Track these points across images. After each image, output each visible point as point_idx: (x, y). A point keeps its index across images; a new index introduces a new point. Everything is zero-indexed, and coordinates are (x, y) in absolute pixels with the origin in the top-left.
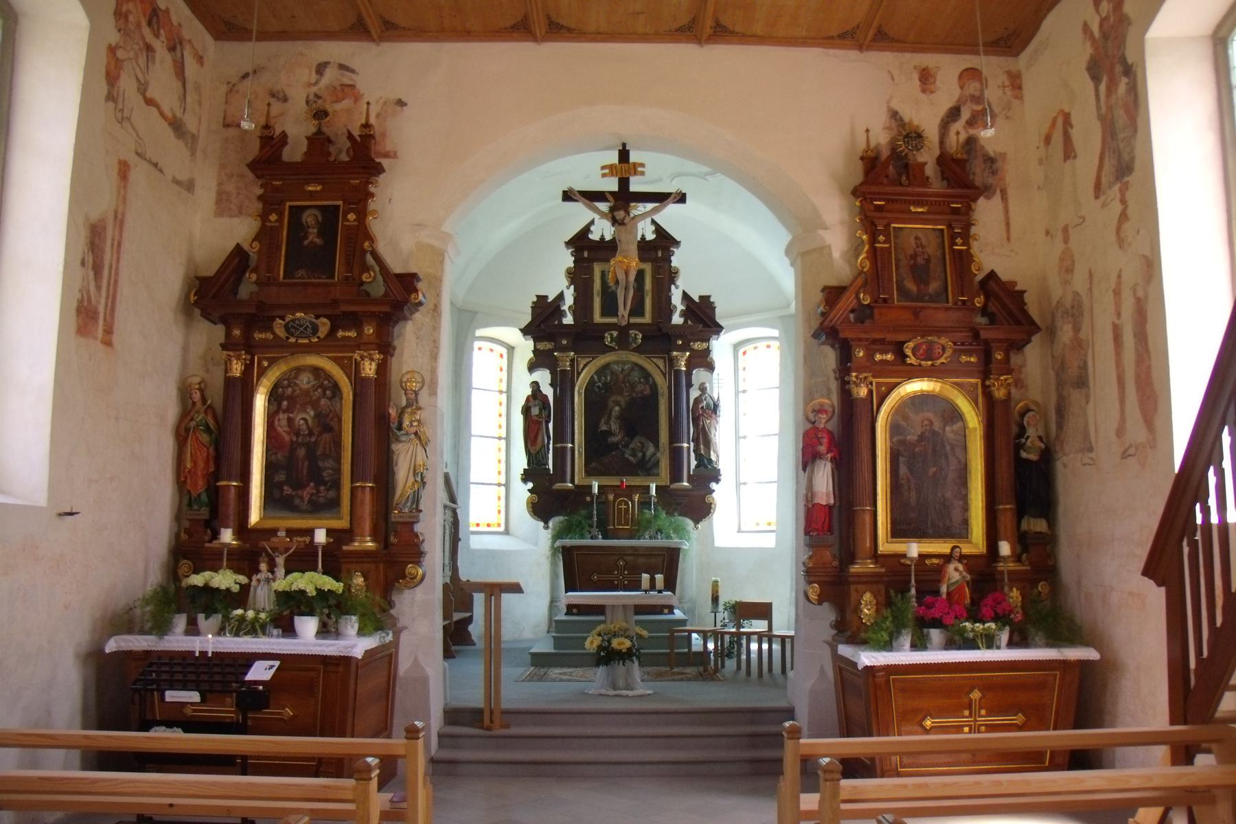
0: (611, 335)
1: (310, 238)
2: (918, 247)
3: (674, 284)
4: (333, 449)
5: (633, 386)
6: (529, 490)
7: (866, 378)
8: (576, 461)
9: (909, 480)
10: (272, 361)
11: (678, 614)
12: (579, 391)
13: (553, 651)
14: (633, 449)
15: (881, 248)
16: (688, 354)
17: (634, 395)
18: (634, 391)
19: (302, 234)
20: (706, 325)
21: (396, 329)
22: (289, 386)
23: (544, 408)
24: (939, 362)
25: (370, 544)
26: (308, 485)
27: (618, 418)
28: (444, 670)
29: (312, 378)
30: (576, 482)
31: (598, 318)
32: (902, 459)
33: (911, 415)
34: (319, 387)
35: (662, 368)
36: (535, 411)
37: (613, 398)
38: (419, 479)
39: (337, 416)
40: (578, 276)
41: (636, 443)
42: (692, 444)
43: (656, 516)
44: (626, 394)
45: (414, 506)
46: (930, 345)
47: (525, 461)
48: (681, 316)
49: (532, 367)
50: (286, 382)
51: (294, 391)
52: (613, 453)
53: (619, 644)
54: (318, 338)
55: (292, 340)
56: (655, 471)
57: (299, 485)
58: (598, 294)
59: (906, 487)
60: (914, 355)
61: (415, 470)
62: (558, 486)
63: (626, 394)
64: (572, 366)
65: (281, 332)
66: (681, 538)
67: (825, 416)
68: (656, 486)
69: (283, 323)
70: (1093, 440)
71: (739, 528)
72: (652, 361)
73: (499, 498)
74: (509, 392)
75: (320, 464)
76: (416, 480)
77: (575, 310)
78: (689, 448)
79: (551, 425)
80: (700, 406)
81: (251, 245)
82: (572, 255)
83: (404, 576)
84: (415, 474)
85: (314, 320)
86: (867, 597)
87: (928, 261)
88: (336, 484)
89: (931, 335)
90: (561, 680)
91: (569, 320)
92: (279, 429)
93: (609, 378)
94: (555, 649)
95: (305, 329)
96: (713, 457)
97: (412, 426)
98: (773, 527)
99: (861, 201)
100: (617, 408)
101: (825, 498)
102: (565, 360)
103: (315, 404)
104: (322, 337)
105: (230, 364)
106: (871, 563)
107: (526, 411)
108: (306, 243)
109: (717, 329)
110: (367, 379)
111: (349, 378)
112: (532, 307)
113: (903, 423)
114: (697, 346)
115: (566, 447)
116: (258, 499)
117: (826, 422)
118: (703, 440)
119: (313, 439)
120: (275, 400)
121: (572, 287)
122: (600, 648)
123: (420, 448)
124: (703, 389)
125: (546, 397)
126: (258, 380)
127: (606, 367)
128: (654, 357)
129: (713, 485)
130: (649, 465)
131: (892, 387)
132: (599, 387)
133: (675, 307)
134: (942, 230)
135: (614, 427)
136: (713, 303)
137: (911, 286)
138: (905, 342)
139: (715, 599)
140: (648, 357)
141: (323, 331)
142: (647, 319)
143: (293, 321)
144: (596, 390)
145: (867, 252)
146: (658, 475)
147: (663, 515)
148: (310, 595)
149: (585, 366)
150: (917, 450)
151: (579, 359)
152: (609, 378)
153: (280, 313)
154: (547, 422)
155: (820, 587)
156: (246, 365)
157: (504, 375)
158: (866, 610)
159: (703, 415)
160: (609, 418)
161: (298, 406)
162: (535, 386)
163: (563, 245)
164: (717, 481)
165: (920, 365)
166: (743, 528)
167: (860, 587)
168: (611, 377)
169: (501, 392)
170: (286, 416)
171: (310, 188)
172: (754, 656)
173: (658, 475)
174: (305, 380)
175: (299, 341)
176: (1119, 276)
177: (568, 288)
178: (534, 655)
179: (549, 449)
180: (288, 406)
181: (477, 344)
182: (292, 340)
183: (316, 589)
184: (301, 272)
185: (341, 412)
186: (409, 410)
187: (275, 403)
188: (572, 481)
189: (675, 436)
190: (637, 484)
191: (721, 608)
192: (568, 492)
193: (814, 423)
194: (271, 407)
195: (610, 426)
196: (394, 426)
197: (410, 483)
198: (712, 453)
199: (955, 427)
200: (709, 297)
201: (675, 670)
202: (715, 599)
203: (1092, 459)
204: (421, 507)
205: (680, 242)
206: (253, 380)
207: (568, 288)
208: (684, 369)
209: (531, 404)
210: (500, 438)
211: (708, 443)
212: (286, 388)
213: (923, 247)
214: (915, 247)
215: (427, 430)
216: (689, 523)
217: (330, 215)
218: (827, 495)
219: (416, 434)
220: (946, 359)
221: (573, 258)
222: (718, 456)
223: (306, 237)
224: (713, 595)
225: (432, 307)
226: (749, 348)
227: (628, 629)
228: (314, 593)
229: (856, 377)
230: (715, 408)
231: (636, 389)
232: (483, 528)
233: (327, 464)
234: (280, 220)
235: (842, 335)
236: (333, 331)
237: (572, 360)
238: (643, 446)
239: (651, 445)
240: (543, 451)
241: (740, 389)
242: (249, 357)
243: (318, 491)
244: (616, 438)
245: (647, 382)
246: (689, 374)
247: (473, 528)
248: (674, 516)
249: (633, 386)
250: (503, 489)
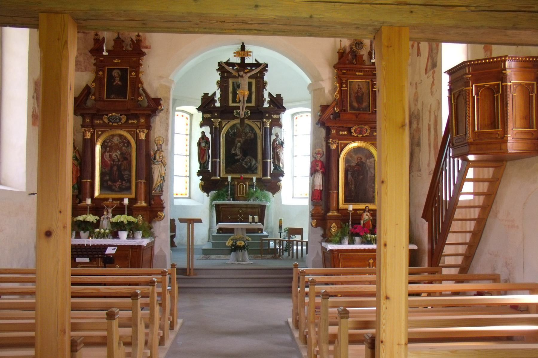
0: (237, 112)
1: (116, 82)
2: (359, 89)
3: (265, 89)
4: (128, 167)
5: (246, 134)
6: (200, 179)
7: (335, 141)
8: (221, 167)
9: (352, 180)
10: (103, 132)
11: (265, 233)
12: (222, 136)
13: (212, 248)
14: (246, 162)
15: (344, 89)
16: (270, 120)
19: (113, 80)
20: (279, 107)
21: (152, 119)
22: (109, 142)
23: (207, 143)
24: (365, 135)
25: (144, 204)
26: (118, 181)
27: (240, 148)
28: (171, 253)
29: (119, 139)
31: (231, 104)
32: (349, 173)
33: (353, 155)
34: (122, 142)
36: (203, 145)
37: (237, 139)
38: (162, 179)
39: (129, 154)
40: (222, 84)
41: (247, 159)
42: (272, 160)
43: (256, 191)
44: (243, 137)
45: (161, 189)
46: (361, 129)
47: (199, 167)
48: (268, 103)
49: (202, 125)
50: (108, 140)
51: (112, 144)
52: (237, 164)
53: (240, 243)
54: (121, 123)
55: (111, 124)
57: (114, 181)
58: (231, 93)
59: (350, 183)
60: (355, 132)
61: (161, 175)
62: (213, 178)
63: (243, 137)
64: (219, 125)
65: (106, 121)
66: (266, 201)
67: (320, 156)
68: (256, 178)
69: (107, 117)
70: (421, 167)
73: (186, 183)
74: (190, 135)
75: (123, 173)
76: (161, 179)
77: (222, 100)
78: (270, 162)
79: (210, 151)
81: (92, 84)
82: (220, 75)
83: (157, 216)
84: (161, 177)
85: (120, 116)
86: (334, 225)
87: (363, 94)
88: (130, 181)
89: (361, 125)
90: (216, 259)
91: (218, 104)
92: (106, 159)
93: (236, 130)
94: (212, 247)
95: (116, 120)
96: (281, 165)
97: (160, 158)
99: (337, 70)
100: (239, 144)
101: (319, 187)
102: (216, 122)
103: (120, 149)
104: (123, 122)
105: (86, 133)
106: (335, 212)
107: (199, 144)
108: (115, 84)
109: (284, 109)
110: (141, 140)
111: (134, 139)
112: (202, 98)
113: (350, 159)
114: (275, 116)
115: (217, 161)
116: (98, 187)
117: (320, 158)
118: (277, 158)
119: (120, 163)
120: (104, 147)
121: (220, 89)
122: (232, 245)
123: (163, 167)
124: (277, 136)
125: (208, 138)
126: (97, 140)
127: (234, 125)
129: (281, 178)
130: (253, 169)
131: (346, 145)
132: (231, 134)
133: (265, 99)
134: (369, 82)
135: (238, 152)
136: (282, 97)
137: (355, 104)
138: (351, 128)
139: (280, 227)
140: (253, 122)
141: (124, 120)
142: (253, 104)
143: (111, 116)
144: (230, 135)
145: (338, 91)
146: (257, 173)
147: (259, 191)
148: (125, 223)
150: (355, 169)
152: (236, 130)
153: (106, 113)
154: (208, 150)
155: (317, 221)
156: (92, 134)
157: (188, 127)
158: (333, 230)
161: (113, 150)
162: (203, 133)
163: (216, 70)
164: (283, 176)
165: (357, 136)
166: (294, 197)
167: (331, 221)
169: (187, 135)
170: (108, 154)
171: (115, 61)
172: (295, 251)
173: (257, 173)
174: (116, 140)
175: (114, 124)
176: (431, 106)
177: (218, 90)
178: (203, 250)
179: (209, 161)
180: (109, 150)
181: (177, 113)
182: (111, 124)
183: (127, 221)
184: (113, 96)
185: (131, 152)
186: (158, 152)
187: (104, 149)
188: (219, 176)
189: (264, 156)
190: (248, 177)
191: (283, 230)
192: (217, 181)
193: (315, 158)
194: (102, 150)
196: (152, 158)
197: (159, 180)
198: (281, 164)
199: (371, 160)
200: (281, 94)
201: (263, 256)
202: (280, 227)
203: (420, 174)
204: (163, 190)
206: (95, 139)
207: (218, 90)
208: (269, 127)
209: (201, 141)
210: (186, 156)
211: (279, 159)
212: (109, 142)
213: (361, 89)
214: (358, 89)
215: (165, 160)
216: (270, 194)
217: (124, 72)
218: (320, 186)
219: (161, 161)
220: (368, 134)
221: (220, 76)
222: (283, 165)
223: (114, 81)
224: (279, 225)
225: (166, 110)
226: (299, 116)
227: (243, 238)
228: (127, 223)
229: (332, 141)
230: (282, 144)
231: (248, 136)
232: (179, 196)
233: (126, 173)
234: (104, 74)
235: (326, 125)
236: (127, 120)
237: (219, 122)
239: (254, 160)
240: (206, 162)
241: (294, 135)
242: (93, 130)
243: (122, 184)
244: (239, 157)
245: (253, 133)
246: (271, 129)
247: (175, 196)
248: (263, 191)
249: (246, 134)
250: (188, 178)
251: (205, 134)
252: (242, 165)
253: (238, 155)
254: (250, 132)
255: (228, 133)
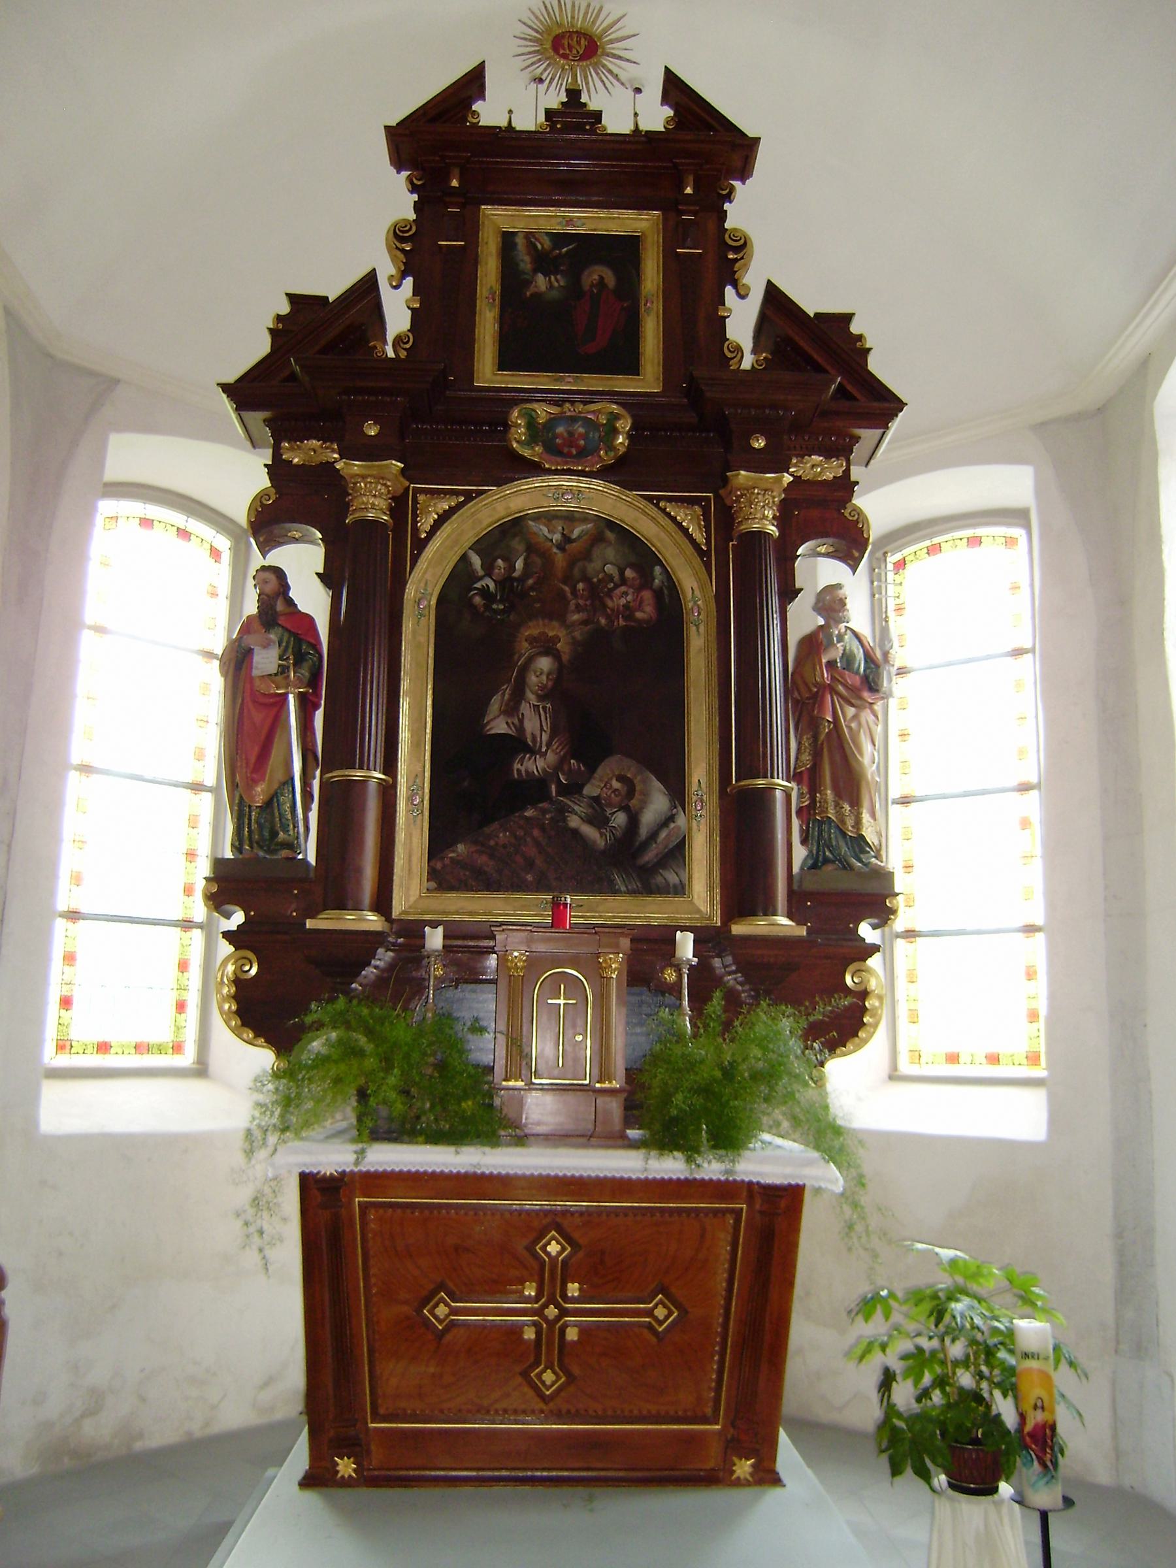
3: (735, 284)
5: (597, 592)
14: (596, 799)
17: (603, 621)
18: (605, 606)
30: (398, 907)
35: (700, 537)
36: (266, 660)
37: (533, 629)
52: (529, 813)
56: (672, 878)
63: (576, 617)
71: (894, 1066)
72: (663, 510)
80: (824, 661)
93: (519, 564)
98: (1040, 1072)
100: (544, 663)
121: (409, 282)
125: (309, 621)
128: (670, 499)
130: (650, 856)
132: (485, 592)
135: (535, 723)
136: (860, 337)
144: (478, 600)
149: (443, 518)
151: (421, 498)
152: (519, 564)
159: (833, 690)
160: (519, 694)
166: (905, 1067)
168: (526, 564)
188: (382, 904)
195: (521, 721)
198: (866, 817)
200: (847, 318)
205: (757, 140)
208: (773, 530)
209: (250, 640)
231: (610, 603)
238: (631, 792)
239: (656, 784)
240: (285, 799)
244: (541, 763)
245: (646, 580)
247: (51, 1057)
249: (597, 592)
251: (284, 587)
252: (565, 820)
253: (532, 751)
254: (624, 581)
255: (460, 577)
